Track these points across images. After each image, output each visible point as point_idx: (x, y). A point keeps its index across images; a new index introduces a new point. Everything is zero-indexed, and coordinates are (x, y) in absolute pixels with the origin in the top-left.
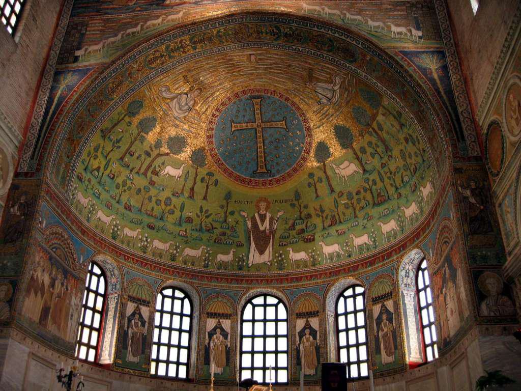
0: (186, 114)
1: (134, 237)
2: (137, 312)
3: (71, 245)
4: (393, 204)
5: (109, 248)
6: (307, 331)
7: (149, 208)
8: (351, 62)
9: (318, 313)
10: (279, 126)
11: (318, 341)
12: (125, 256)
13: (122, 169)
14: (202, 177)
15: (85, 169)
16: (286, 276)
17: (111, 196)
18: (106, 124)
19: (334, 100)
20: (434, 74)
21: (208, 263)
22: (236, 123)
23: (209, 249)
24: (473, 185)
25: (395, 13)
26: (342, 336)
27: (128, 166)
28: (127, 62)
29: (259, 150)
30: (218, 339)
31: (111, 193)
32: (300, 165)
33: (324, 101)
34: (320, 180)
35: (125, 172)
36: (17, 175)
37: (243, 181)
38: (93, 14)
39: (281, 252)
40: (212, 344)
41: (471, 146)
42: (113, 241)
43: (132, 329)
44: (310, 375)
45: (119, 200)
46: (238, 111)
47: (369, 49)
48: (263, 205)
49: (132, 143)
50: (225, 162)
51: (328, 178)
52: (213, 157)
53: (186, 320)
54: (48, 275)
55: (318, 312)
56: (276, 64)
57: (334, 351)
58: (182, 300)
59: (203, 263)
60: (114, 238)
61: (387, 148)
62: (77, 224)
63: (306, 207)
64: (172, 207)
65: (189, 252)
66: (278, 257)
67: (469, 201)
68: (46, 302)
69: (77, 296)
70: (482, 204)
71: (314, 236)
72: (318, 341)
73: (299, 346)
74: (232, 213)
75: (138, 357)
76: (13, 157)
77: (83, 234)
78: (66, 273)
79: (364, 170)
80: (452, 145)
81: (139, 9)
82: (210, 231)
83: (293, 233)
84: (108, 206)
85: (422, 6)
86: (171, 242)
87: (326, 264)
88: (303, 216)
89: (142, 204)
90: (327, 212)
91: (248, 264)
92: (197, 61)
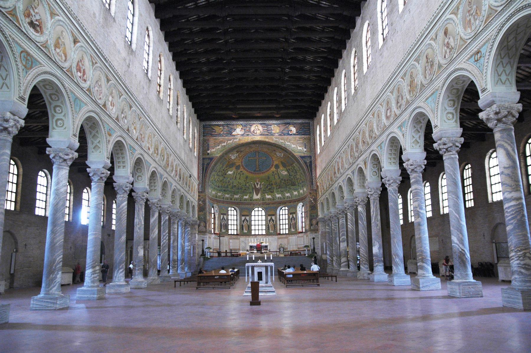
2: (223, 218)
4: (297, 187)
7: (224, 185)
9: (275, 215)
24: (313, 197)
26: (281, 221)
32: (270, 169)
36: (199, 192)
37: (251, 173)
48: (258, 180)
61: (296, 172)
65: (236, 196)
74: (248, 183)
79: (290, 175)
83: (267, 189)
84: (214, 189)
90: (277, 184)
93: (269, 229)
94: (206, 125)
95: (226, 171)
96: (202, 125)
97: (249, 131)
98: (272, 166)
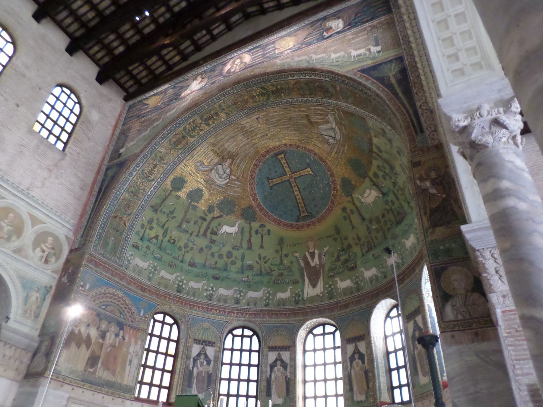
0: (228, 180)
1: (199, 289)
2: (202, 353)
3: (128, 302)
5: (174, 300)
6: (357, 356)
7: (213, 262)
8: (330, 97)
10: (307, 173)
11: (366, 365)
12: (190, 305)
13: (182, 234)
14: (255, 230)
15: (141, 239)
16: (336, 304)
17: (174, 257)
18: (155, 201)
19: (338, 137)
20: (391, 79)
21: (269, 302)
22: (272, 179)
23: (269, 289)
24: (433, 175)
25: (357, 39)
27: (187, 231)
28: (153, 148)
29: (297, 198)
30: (279, 370)
31: (173, 255)
32: (334, 202)
33: (331, 141)
34: (352, 212)
35: (185, 237)
36: (71, 251)
37: (291, 227)
38: (136, 119)
39: (330, 283)
40: (273, 376)
41: (431, 136)
42: (177, 294)
43: (198, 368)
44: (361, 401)
45: (183, 259)
46: (270, 169)
47: (334, 79)
48: (311, 244)
49: (186, 212)
50: (272, 213)
51: (357, 208)
52: (261, 211)
53: (255, 356)
54: (95, 328)
55: (364, 335)
56: (280, 120)
57: (385, 375)
58: (251, 337)
59: (264, 303)
60: (179, 291)
62: (135, 284)
63: (346, 238)
64: (233, 258)
65: (252, 294)
66: (328, 288)
67: (429, 193)
68: (93, 352)
69: (136, 343)
70: (444, 193)
71: (355, 264)
72: (366, 365)
73: (350, 371)
74: (286, 256)
75: (203, 393)
76: (67, 237)
77: (144, 292)
78: (121, 326)
79: (384, 194)
80: (410, 140)
81: (164, 106)
82: (270, 274)
83: (339, 264)
85: (383, 25)
86: (235, 288)
87: (367, 288)
88: (345, 247)
89: (206, 260)
90: (363, 239)
91: (303, 298)
92: (217, 135)
93: (351, 389)
94: (134, 104)
95: (214, 224)
96: (127, 108)
97: (221, 74)
98: (335, 189)
